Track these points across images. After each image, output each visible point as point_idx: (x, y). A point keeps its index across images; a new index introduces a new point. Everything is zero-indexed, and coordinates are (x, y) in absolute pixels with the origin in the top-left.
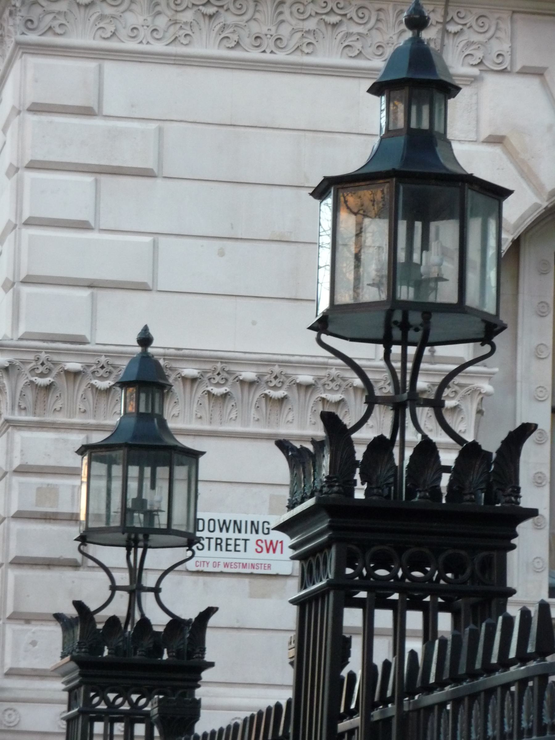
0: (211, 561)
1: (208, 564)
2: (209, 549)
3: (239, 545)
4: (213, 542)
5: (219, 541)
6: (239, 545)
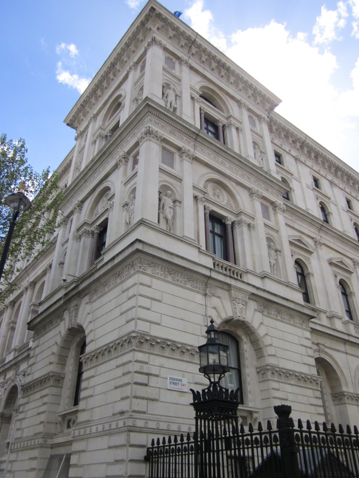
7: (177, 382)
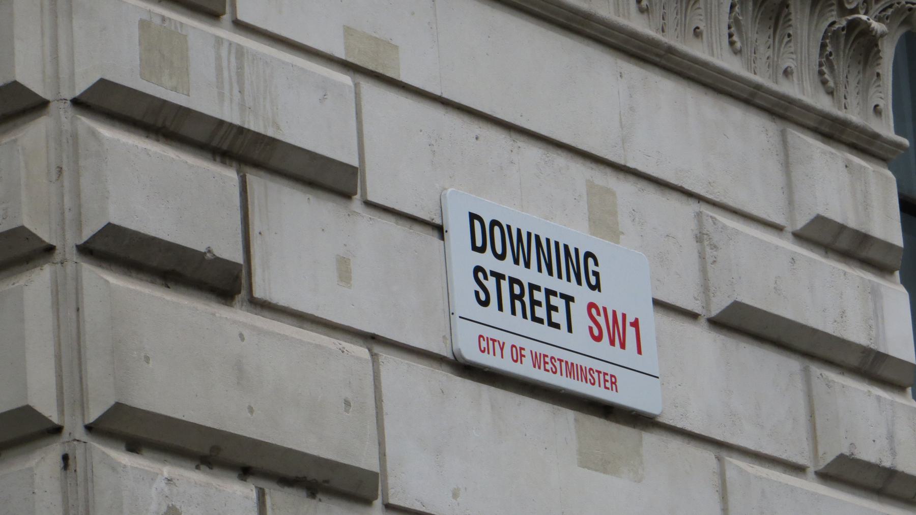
1: (502, 349)
3: (556, 309)
4: (505, 284)
5: (517, 290)
6: (556, 309)
7: (545, 281)
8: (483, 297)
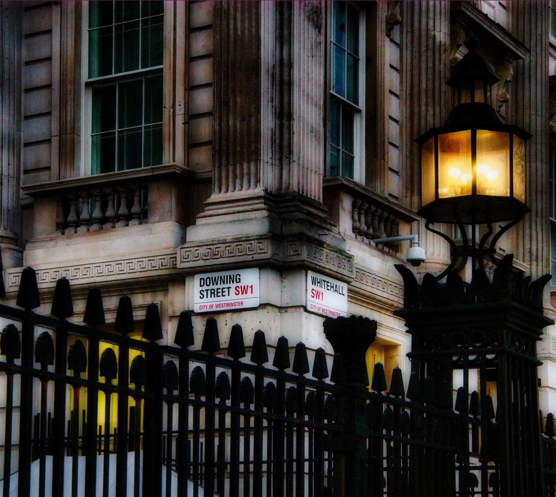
0: (208, 304)
2: (207, 297)
4: (209, 292)
5: (213, 291)
7: (223, 286)
8: (202, 296)
